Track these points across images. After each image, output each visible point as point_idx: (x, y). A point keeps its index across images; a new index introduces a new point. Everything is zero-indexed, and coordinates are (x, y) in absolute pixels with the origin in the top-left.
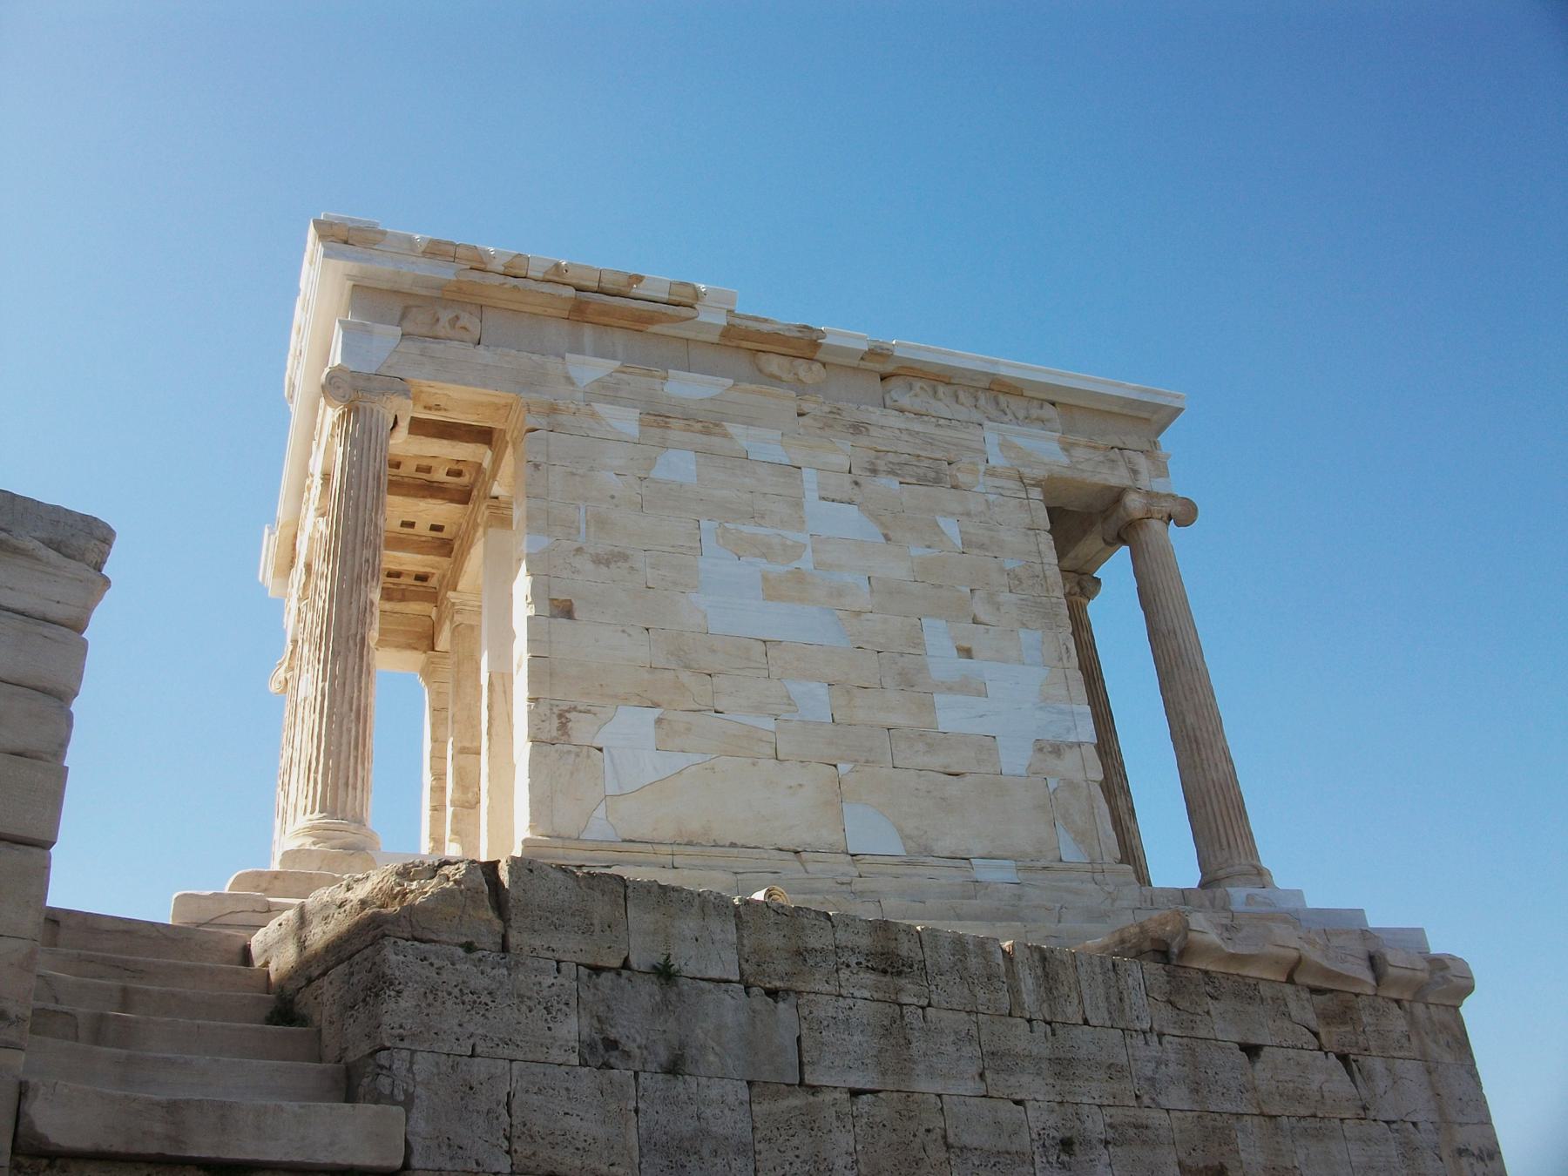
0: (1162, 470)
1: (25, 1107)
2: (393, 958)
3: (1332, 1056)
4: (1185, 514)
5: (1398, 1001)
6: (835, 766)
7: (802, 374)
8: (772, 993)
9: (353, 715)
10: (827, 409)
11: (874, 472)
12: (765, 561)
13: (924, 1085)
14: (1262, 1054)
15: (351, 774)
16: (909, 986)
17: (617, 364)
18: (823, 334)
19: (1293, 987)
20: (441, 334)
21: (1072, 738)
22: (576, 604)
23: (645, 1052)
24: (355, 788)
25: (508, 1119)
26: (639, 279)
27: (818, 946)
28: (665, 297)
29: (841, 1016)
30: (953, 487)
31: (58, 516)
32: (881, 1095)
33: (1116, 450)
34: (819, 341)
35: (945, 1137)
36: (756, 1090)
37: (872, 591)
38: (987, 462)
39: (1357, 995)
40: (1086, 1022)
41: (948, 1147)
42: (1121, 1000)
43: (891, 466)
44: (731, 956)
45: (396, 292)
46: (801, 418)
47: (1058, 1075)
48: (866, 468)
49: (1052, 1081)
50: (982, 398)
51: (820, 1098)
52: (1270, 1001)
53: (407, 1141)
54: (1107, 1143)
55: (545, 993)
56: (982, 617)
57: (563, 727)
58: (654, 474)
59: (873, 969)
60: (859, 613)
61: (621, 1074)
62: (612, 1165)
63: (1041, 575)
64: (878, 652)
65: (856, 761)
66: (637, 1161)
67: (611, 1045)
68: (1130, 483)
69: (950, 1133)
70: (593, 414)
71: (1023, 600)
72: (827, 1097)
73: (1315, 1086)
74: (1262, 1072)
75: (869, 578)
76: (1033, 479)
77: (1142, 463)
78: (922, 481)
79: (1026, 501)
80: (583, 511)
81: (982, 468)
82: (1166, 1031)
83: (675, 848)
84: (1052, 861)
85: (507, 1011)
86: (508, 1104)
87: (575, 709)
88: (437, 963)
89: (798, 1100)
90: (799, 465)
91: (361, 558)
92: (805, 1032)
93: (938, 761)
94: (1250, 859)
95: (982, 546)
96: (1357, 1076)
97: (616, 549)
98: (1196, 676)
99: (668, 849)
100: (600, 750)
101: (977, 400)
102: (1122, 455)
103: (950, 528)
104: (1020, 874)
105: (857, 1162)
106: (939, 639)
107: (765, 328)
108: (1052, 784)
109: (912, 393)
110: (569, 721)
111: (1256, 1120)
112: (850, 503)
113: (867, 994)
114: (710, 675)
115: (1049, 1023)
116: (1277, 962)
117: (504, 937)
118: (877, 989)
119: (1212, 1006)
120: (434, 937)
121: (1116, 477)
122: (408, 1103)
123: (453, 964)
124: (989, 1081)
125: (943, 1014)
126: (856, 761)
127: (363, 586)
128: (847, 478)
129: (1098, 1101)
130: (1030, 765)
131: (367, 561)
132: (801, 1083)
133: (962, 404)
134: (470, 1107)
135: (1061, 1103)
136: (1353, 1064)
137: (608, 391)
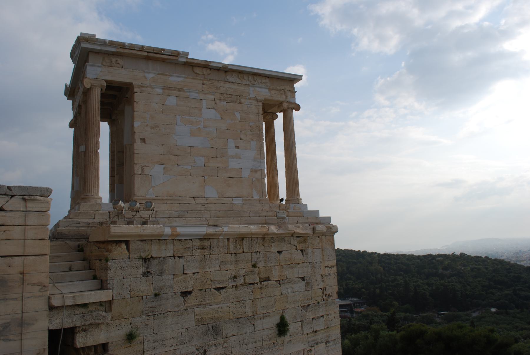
0: (294, 97)
1: (50, 301)
2: (109, 264)
4: (298, 108)
5: (318, 236)
6: (204, 177)
7: (205, 73)
8: (179, 257)
9: (95, 170)
11: (220, 100)
12: (192, 126)
13: (208, 270)
14: (282, 252)
15: (95, 184)
16: (207, 251)
19: (293, 237)
21: (260, 168)
22: (146, 139)
23: (155, 272)
24: (96, 187)
25: (130, 288)
26: (163, 50)
27: (189, 246)
28: (171, 54)
30: (240, 103)
31: (42, 189)
32: (199, 273)
33: (283, 90)
34: (210, 65)
35: (211, 279)
36: (175, 276)
37: (217, 133)
38: (249, 96)
39: (308, 236)
40: (243, 252)
41: (211, 281)
42: (252, 246)
43: (225, 98)
44: (171, 252)
46: (204, 86)
47: (236, 264)
49: (234, 265)
50: (250, 77)
51: (187, 275)
52: (287, 241)
53: (113, 295)
55: (137, 265)
56: (243, 138)
57: (143, 170)
58: (165, 103)
59: (200, 249)
60: (212, 139)
61: (150, 277)
62: (148, 293)
63: (258, 126)
65: (209, 176)
66: (152, 292)
67: (148, 272)
68: (285, 100)
71: (253, 133)
72: (188, 275)
73: (294, 257)
74: (282, 256)
75: (216, 129)
76: (260, 100)
77: (289, 94)
78: (232, 102)
80: (148, 114)
82: (261, 251)
85: (130, 269)
86: (130, 286)
87: (145, 166)
88: (117, 263)
89: (183, 276)
90: (202, 99)
91: (95, 130)
92: (185, 263)
94: (297, 196)
96: (304, 254)
98: (292, 151)
100: (151, 175)
102: (284, 91)
105: (193, 286)
106: (231, 143)
107: (196, 62)
108: (254, 179)
109: (232, 77)
110: (144, 169)
111: (278, 266)
112: (213, 109)
113: (198, 254)
115: (235, 254)
116: (288, 233)
117: (129, 256)
118: (200, 253)
119: (273, 244)
120: (116, 258)
121: (282, 98)
123: (120, 263)
124: (221, 267)
125: (213, 255)
126: (209, 176)
127: (96, 137)
128: (214, 102)
129: (243, 268)
130: (249, 175)
131: (96, 130)
132: (184, 273)
133: (245, 79)
134: (123, 288)
136: (304, 252)
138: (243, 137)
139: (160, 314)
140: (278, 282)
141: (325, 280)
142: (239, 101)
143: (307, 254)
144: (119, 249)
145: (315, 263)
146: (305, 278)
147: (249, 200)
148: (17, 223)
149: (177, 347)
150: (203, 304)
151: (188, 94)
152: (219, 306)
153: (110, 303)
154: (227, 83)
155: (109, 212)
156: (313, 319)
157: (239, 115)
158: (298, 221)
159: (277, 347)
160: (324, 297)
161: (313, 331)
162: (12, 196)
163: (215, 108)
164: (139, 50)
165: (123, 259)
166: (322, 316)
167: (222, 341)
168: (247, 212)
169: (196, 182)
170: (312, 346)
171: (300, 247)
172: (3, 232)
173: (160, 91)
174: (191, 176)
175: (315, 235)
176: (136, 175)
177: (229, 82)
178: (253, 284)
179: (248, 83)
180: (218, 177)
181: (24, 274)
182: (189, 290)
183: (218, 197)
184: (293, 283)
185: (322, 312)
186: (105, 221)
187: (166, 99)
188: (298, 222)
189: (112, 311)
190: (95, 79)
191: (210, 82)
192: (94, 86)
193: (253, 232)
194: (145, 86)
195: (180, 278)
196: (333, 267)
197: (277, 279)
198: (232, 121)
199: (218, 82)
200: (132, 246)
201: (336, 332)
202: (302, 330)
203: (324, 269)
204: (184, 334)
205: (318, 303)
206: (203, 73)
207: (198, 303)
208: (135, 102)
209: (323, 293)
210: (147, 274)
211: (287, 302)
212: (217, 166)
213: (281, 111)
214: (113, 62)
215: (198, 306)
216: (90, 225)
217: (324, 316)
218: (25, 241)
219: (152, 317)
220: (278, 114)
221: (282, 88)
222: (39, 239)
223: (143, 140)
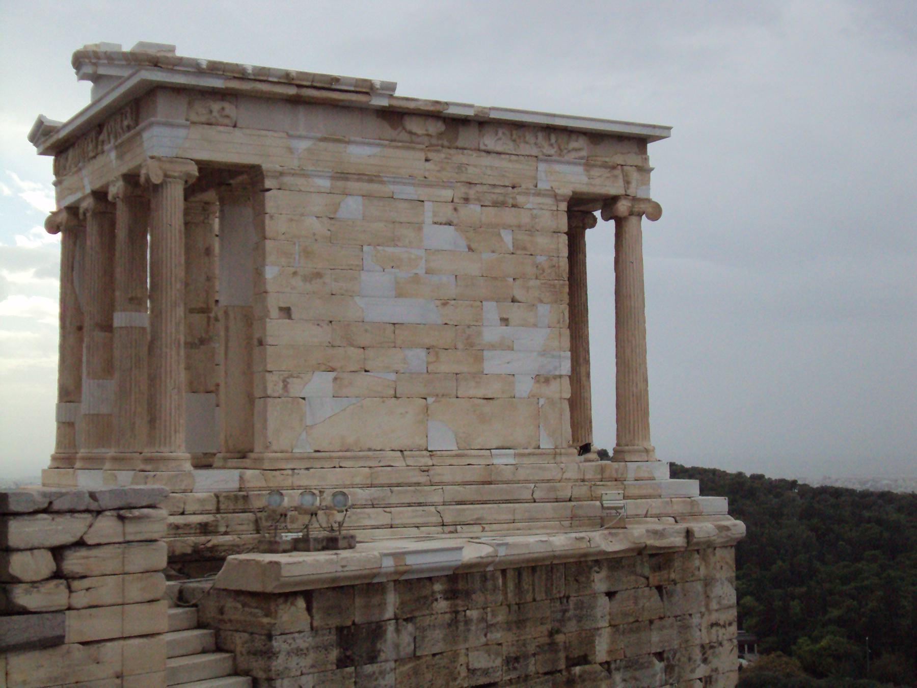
0: (646, 182)
3: (653, 588)
4: (655, 213)
6: (425, 399)
10: (443, 156)
11: (466, 200)
14: (618, 596)
20: (213, 121)
21: (557, 373)
22: (292, 309)
26: (337, 80)
28: (352, 89)
29: (432, 624)
30: (514, 206)
33: (619, 167)
38: (536, 186)
40: (534, 600)
46: (427, 164)
48: (462, 198)
50: (540, 135)
51: (421, 660)
56: (518, 297)
57: (285, 387)
58: (338, 215)
63: (557, 265)
64: (456, 326)
65: (437, 395)
69: (470, 664)
72: (423, 660)
75: (456, 276)
78: (495, 204)
79: (556, 212)
80: (297, 247)
81: (533, 191)
83: (340, 454)
84: (535, 448)
90: (421, 199)
93: (481, 392)
95: (525, 249)
96: (665, 596)
97: (317, 270)
100: (304, 399)
101: (537, 139)
102: (622, 170)
103: (507, 237)
106: (491, 311)
107: (412, 105)
108: (542, 401)
109: (497, 137)
110: (288, 383)
112: (450, 225)
114: (363, 348)
126: (437, 395)
128: (450, 206)
130: (531, 391)
133: (527, 143)
135: (518, 641)
136: (664, 591)
138: (518, 294)
140: (606, 666)
141: (710, 658)
142: (510, 201)
143: (671, 594)
144: (293, 608)
145: (688, 617)
146: (665, 655)
147: (529, 454)
151: (390, 188)
154: (483, 154)
155: (217, 496)
158: (647, 511)
162: (99, 512)
163: (455, 222)
164: (279, 83)
165: (299, 632)
168: (528, 489)
169: (407, 412)
171: (655, 579)
172: (85, 591)
173: (325, 183)
174: (395, 397)
175: (690, 548)
176: (269, 399)
177: (488, 152)
179: (535, 151)
180: (457, 397)
181: (125, 678)
183: (455, 448)
184: (636, 666)
186: (213, 521)
187: (339, 204)
188: (649, 513)
190: (174, 160)
191: (443, 156)
192: (169, 177)
193: (557, 554)
194: (290, 173)
196: (730, 624)
198: (494, 254)
199: (463, 154)
203: (708, 632)
206: (426, 130)
208: (267, 215)
212: (455, 372)
213: (611, 218)
214: (215, 114)
216: (180, 531)
218: (126, 607)
220: (598, 214)
222: (148, 600)
223: (287, 312)
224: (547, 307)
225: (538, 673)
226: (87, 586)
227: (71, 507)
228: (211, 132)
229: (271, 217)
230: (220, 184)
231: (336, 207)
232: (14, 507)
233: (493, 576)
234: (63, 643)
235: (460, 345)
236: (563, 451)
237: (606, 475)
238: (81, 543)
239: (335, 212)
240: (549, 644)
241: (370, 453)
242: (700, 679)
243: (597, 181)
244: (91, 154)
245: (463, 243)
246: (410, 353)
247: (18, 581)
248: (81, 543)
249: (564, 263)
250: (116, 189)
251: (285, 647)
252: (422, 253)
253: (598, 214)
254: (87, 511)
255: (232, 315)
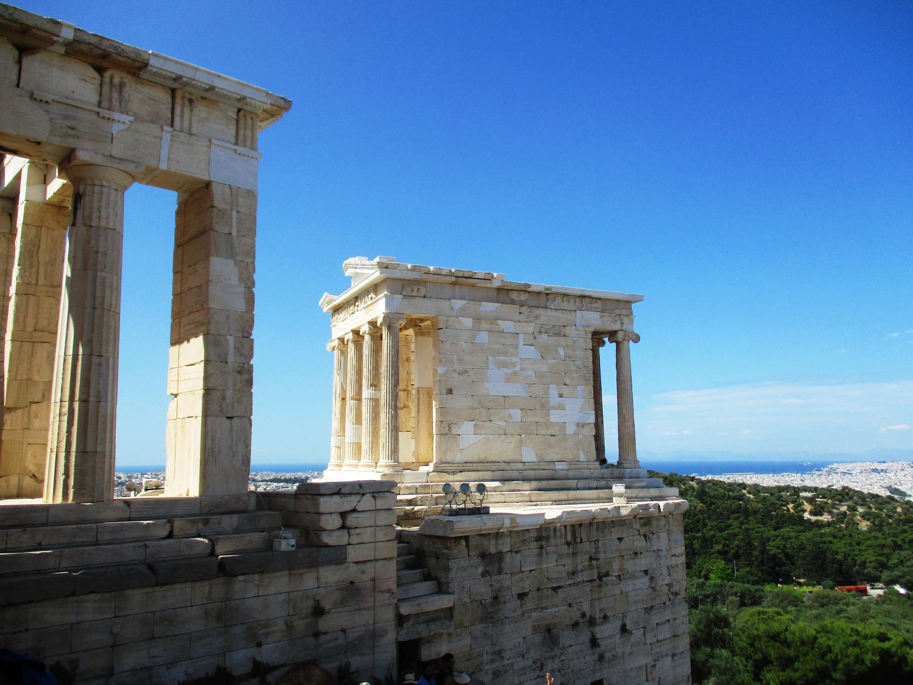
0: (631, 322)
4: (637, 339)
11: (541, 333)
13: (545, 566)
14: (624, 540)
17: (466, 301)
18: (529, 286)
20: (414, 295)
26: (476, 273)
40: (581, 542)
41: (548, 579)
44: (509, 546)
45: (400, 279)
54: (582, 571)
56: (567, 383)
58: (477, 341)
61: (488, 578)
70: (459, 322)
72: (525, 573)
74: (622, 545)
89: (520, 575)
93: (549, 432)
95: (570, 357)
99: (474, 465)
100: (459, 435)
101: (575, 302)
104: (568, 466)
106: (553, 391)
107: (513, 285)
108: (580, 436)
117: (468, 554)
119: (613, 530)
122: (454, 594)
137: (463, 313)
138: (568, 381)
139: (498, 621)
141: (672, 573)
143: (650, 540)
148: (368, 524)
149: (514, 660)
150: (540, 608)
152: (556, 609)
153: (451, 610)
156: (657, 624)
157: (563, 352)
159: (618, 660)
160: (670, 595)
161: (657, 641)
162: (363, 495)
165: (463, 558)
166: (668, 621)
167: (559, 654)
170: (655, 661)
178: (590, 581)
179: (574, 308)
182: (526, 591)
185: (668, 615)
189: (454, 619)
191: (528, 310)
195: (517, 576)
196: (682, 555)
197: (617, 574)
200: (472, 542)
201: (684, 643)
202: (645, 639)
204: (521, 644)
205: (664, 603)
207: (536, 607)
209: (669, 590)
210: (484, 574)
211: (628, 603)
215: (534, 610)
217: (671, 621)
219: (491, 624)
220: (606, 339)
221: (618, 312)
224: (583, 387)
225: (584, 581)
226: (357, 532)
227: (350, 492)
228: (413, 301)
229: (442, 342)
230: (416, 326)
231: (475, 337)
232: (322, 491)
233: (560, 529)
234: (345, 563)
235: (538, 407)
236: (592, 463)
237: (614, 476)
238: (354, 510)
239: (474, 339)
240: (589, 565)
241: (492, 464)
242: (667, 585)
243: (607, 324)
244: (352, 312)
245: (539, 355)
246: (512, 411)
247: (325, 530)
248: (354, 510)
249: (591, 366)
250: (365, 329)
251: (455, 565)
252: (517, 360)
253: (606, 339)
254: (358, 493)
255: (421, 392)
